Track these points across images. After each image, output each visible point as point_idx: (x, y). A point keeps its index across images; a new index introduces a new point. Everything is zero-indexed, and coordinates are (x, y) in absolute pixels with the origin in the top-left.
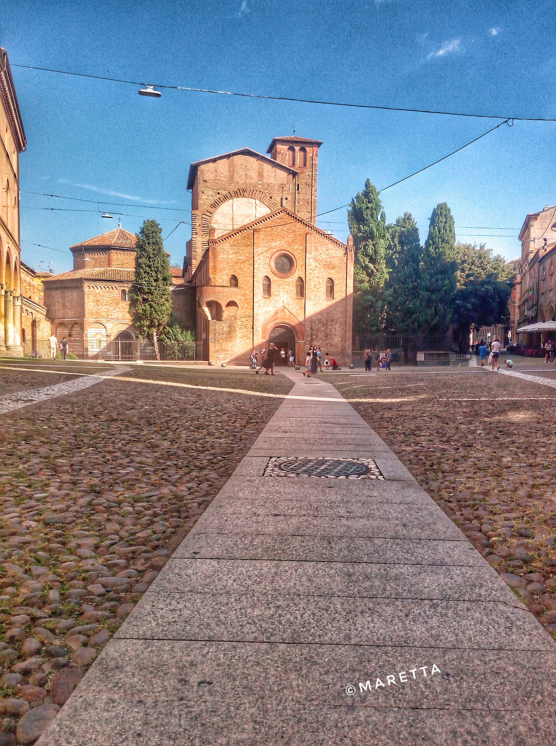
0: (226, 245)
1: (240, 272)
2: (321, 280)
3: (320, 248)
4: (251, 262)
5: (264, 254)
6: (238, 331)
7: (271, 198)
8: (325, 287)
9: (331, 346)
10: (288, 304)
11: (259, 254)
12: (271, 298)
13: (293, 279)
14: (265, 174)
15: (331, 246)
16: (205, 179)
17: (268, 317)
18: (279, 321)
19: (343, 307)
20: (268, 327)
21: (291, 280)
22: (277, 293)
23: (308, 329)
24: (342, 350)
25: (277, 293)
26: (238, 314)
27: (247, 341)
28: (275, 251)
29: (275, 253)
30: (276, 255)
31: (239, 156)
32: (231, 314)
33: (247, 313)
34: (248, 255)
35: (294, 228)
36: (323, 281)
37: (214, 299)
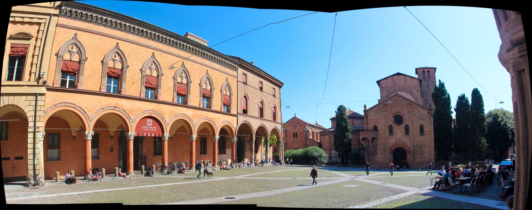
0: (372, 113)
1: (378, 123)
2: (417, 126)
3: (415, 111)
4: (383, 118)
5: (389, 115)
6: (378, 151)
7: (411, 91)
8: (419, 129)
9: (424, 158)
10: (402, 138)
11: (387, 115)
12: (393, 135)
13: (403, 126)
14: (407, 82)
15: (421, 109)
16: (383, 86)
17: (392, 144)
18: (397, 146)
19: (429, 138)
20: (393, 149)
21: (403, 126)
22: (396, 133)
23: (412, 150)
24: (429, 160)
25: (396, 133)
26: (378, 143)
27: (383, 156)
28: (394, 113)
29: (394, 114)
30: (395, 115)
31: (396, 76)
32: (375, 143)
33: (382, 143)
34: (381, 116)
35: (402, 102)
36: (418, 126)
37: (365, 136)
